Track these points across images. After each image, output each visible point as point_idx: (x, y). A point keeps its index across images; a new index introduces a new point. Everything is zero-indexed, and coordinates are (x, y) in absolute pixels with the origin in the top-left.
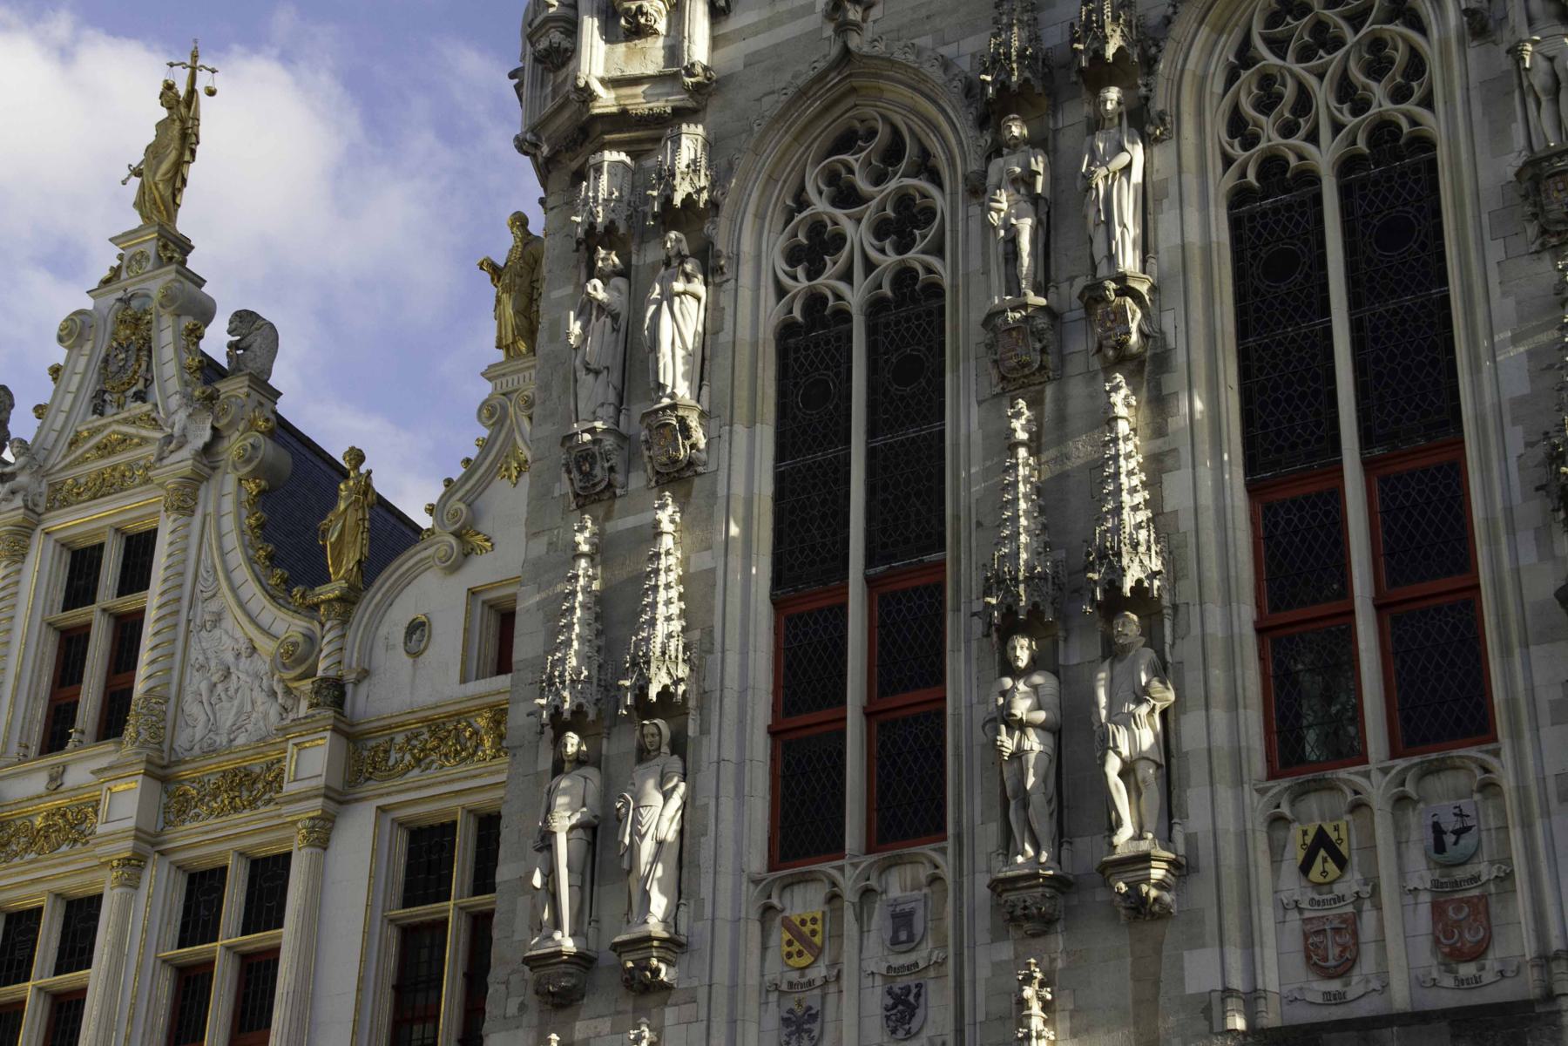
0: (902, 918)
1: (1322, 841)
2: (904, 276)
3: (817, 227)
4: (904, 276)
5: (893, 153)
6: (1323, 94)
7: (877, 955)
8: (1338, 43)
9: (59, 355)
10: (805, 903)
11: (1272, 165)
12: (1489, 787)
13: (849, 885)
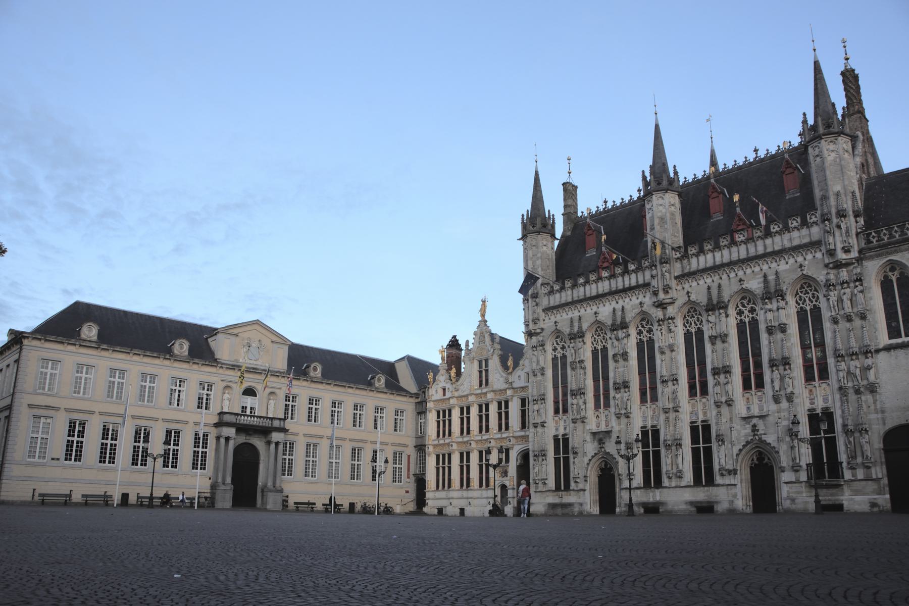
0: (565, 421)
1: (598, 416)
3: (555, 347)
5: (562, 340)
9: (474, 336)
10: (556, 418)
11: (595, 347)
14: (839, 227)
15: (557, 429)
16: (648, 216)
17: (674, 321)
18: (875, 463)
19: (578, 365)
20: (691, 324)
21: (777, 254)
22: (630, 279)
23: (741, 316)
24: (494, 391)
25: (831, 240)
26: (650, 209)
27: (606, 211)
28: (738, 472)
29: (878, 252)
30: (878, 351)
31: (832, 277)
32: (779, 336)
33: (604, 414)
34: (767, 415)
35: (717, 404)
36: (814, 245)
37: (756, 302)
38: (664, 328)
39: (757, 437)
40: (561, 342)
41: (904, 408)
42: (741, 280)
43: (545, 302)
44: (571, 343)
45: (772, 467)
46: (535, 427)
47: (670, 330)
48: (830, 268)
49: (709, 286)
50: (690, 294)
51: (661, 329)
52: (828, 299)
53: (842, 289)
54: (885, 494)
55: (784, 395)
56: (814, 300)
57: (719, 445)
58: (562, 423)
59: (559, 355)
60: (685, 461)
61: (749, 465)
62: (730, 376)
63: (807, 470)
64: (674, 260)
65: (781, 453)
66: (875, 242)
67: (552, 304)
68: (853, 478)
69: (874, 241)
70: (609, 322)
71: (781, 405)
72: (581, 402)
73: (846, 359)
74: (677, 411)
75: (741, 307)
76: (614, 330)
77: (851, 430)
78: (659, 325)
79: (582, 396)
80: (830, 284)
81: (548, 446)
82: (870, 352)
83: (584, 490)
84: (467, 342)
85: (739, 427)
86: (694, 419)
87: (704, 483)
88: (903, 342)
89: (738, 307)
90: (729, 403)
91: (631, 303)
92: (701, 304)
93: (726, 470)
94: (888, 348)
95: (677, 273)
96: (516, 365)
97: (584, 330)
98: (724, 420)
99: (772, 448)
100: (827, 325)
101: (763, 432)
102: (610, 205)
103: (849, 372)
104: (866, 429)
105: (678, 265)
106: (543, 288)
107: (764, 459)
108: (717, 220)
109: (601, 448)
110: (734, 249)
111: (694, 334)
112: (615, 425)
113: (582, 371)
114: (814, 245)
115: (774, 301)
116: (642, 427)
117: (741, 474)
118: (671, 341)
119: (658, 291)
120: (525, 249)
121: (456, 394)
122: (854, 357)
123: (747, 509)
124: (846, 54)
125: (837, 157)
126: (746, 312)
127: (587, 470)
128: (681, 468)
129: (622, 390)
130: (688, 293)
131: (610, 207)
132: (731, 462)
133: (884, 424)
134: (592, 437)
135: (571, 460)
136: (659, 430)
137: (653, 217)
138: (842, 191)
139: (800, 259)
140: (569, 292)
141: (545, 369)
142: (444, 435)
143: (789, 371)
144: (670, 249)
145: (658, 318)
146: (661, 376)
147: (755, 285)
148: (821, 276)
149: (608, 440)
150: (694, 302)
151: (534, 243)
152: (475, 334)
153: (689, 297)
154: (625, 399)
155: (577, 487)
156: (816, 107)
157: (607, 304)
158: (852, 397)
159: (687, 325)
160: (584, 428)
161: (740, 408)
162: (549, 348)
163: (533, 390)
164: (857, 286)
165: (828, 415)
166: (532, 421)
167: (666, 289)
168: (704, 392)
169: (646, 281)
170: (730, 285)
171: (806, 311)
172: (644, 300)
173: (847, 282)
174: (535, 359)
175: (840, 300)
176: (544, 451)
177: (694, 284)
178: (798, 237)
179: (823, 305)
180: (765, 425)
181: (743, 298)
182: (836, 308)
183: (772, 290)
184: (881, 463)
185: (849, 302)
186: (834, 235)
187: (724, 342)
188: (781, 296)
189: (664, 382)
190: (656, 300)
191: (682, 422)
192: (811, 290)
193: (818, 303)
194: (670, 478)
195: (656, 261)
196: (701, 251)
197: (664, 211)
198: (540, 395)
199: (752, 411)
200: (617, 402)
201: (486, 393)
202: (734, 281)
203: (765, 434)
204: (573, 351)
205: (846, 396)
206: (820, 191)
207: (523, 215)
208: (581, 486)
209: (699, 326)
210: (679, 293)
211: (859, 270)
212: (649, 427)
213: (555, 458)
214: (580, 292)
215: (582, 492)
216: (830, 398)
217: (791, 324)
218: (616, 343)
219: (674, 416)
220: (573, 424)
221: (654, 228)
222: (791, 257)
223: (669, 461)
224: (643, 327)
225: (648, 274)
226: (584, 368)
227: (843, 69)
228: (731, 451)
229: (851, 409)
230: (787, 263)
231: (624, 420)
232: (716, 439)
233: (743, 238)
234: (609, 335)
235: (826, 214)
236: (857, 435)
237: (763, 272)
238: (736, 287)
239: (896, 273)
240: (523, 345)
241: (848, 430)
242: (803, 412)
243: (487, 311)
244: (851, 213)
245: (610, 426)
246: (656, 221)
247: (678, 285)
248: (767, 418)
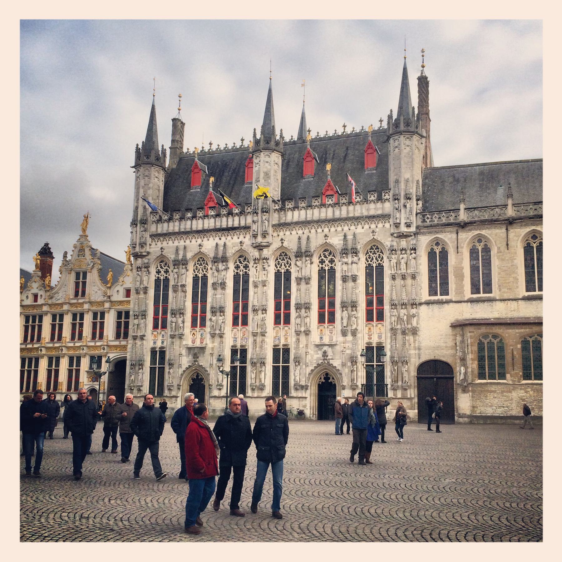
0: (163, 335)
1: (194, 333)
2: (166, 277)
4: (166, 277)
5: (166, 264)
6: (201, 269)
7: (161, 338)
8: (202, 265)
9: (74, 249)
10: (155, 333)
12: (205, 331)
13: (159, 332)
14: (405, 206)
15: (155, 343)
16: (255, 169)
17: (268, 261)
18: (410, 387)
19: (180, 288)
20: (281, 265)
21: (357, 220)
22: (233, 220)
23: (322, 265)
24: (91, 303)
25: (398, 216)
26: (258, 163)
27: (210, 153)
28: (309, 387)
29: (429, 230)
30: (421, 304)
31: (395, 244)
32: (350, 284)
33: (200, 334)
34: (335, 345)
35: (297, 332)
36: (384, 217)
37: (335, 255)
38: (259, 267)
39: (326, 362)
40: (165, 267)
41: (434, 348)
42: (326, 236)
43: (153, 228)
44: (174, 268)
46: (135, 338)
47: (264, 268)
49: (299, 237)
50: (283, 241)
51: (256, 267)
52: (390, 260)
53: (401, 254)
54: (415, 409)
55: (349, 330)
56: (379, 260)
57: (296, 366)
58: (160, 338)
59: (162, 278)
60: (266, 376)
61: (318, 383)
62: (309, 311)
63: (362, 388)
64: (273, 210)
65: (343, 375)
66: (428, 222)
67: (159, 231)
68: (394, 397)
69: (428, 221)
70: (212, 255)
71: (347, 337)
72: (180, 320)
73: (398, 307)
74: (265, 336)
75: (323, 258)
76: (215, 262)
77: (396, 361)
78: (255, 263)
79: (181, 315)
80: (393, 249)
81: (145, 357)
82: (416, 304)
83: (177, 397)
84: (66, 253)
85: (312, 352)
86: (277, 342)
88: (439, 299)
89: (321, 257)
90: (307, 333)
91: (232, 241)
92: (293, 250)
93: (300, 385)
94: (428, 303)
95: (275, 222)
96: (115, 280)
97: (188, 259)
98: (301, 346)
99: (337, 370)
100: (387, 280)
101: (331, 358)
102: (214, 148)
103: (399, 317)
104: (407, 361)
105: (276, 215)
106: (152, 216)
107: (329, 378)
108: (308, 181)
109: (195, 361)
110: (323, 210)
111: (283, 274)
112: (209, 343)
113: (183, 294)
114: (384, 217)
115: (350, 256)
116: (232, 346)
117: (310, 388)
118: (265, 279)
119: (257, 234)
120: (137, 178)
121: (50, 302)
122: (403, 307)
123: (313, 417)
124: (423, 63)
125: (410, 151)
126: (327, 262)
127: (181, 380)
128: (263, 382)
129: (218, 314)
130: (282, 240)
131: (214, 150)
132: (304, 379)
133: (419, 358)
134: (187, 351)
135: (167, 370)
136: (247, 349)
137: (258, 172)
138: (410, 179)
139: (373, 226)
140: (177, 223)
141: (148, 289)
142: (32, 339)
143: (355, 313)
144: (271, 201)
145: (255, 257)
146: (253, 306)
147: (336, 241)
148: (387, 242)
149: (202, 355)
150: (286, 248)
151: (147, 173)
152: (75, 247)
153: (282, 243)
154: (220, 322)
155: (170, 394)
156: (400, 108)
157: (211, 239)
158: (400, 337)
159: (278, 266)
160: (180, 343)
161: (315, 337)
162: (153, 270)
163: (134, 307)
164: (412, 254)
165: (380, 348)
166: (131, 333)
167: (264, 235)
168: (287, 321)
169: (247, 225)
170: (316, 238)
171: (373, 267)
172: (244, 240)
173: (405, 250)
174: (139, 278)
175: (398, 263)
176: (142, 361)
177: (288, 233)
178: (374, 209)
179: (386, 264)
180: (333, 352)
181: (325, 251)
182: (395, 268)
183: (350, 247)
184: (415, 387)
185: (405, 265)
186: (400, 212)
188: (356, 253)
189: (255, 311)
190: (254, 242)
191: (266, 345)
192: (378, 252)
193: (382, 262)
194: (253, 390)
195: (258, 209)
196: (296, 207)
197: (269, 167)
198: (142, 311)
200: (212, 323)
201: (83, 303)
202: (321, 236)
203: (332, 359)
204: (176, 276)
205: (394, 335)
206: (394, 176)
207: (137, 145)
208: (174, 393)
209: (288, 268)
210: (274, 238)
211: (414, 242)
212: (239, 347)
213: (151, 368)
214: (187, 225)
215: (174, 399)
216: (383, 336)
217: (360, 276)
218: (216, 274)
219: (261, 340)
220: (171, 339)
221: (259, 181)
222: (366, 224)
223: (253, 376)
224: (240, 262)
225: (249, 219)
226: (185, 292)
227: (419, 75)
228: (304, 371)
229: (397, 345)
230: (363, 228)
231: (217, 339)
232: (294, 360)
233: (332, 202)
234: (210, 266)
235: (397, 195)
236: (400, 364)
237: (344, 231)
238: (321, 241)
239: (440, 247)
240: (124, 263)
241: (394, 361)
242: (362, 345)
243: (88, 226)
244: (414, 197)
245: (204, 343)
246: (262, 175)
247: (274, 231)
248: (335, 347)
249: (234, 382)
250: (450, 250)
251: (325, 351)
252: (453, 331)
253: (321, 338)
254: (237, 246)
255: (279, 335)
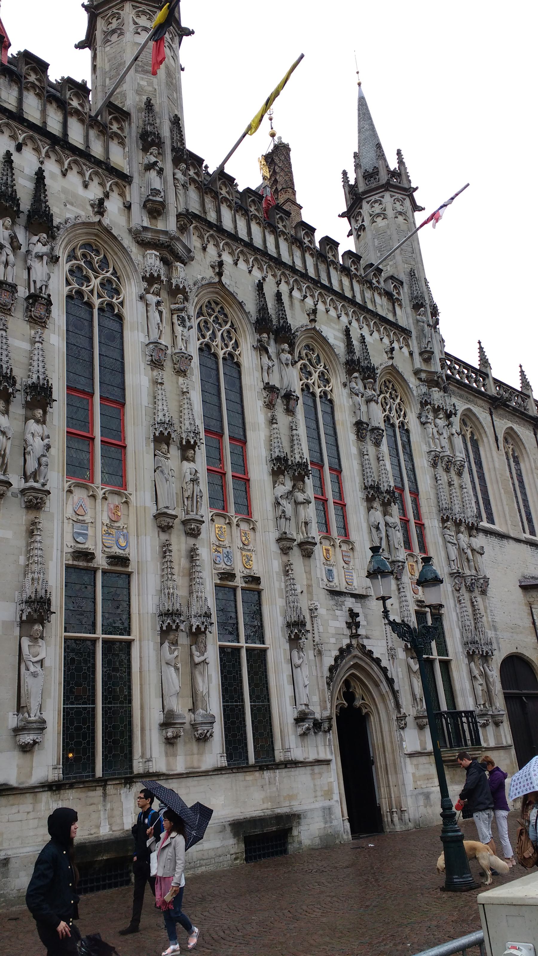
45: (367, 714)
48: (420, 379)
51: (158, 303)
78: (147, 291)
87: (252, 759)
103: (461, 551)
153: (220, 274)
187: (290, 411)
190: (145, 224)
194: (170, 742)
199: (336, 580)
249: (78, 712)
250: (485, 439)
251: (351, 610)
252: (525, 596)
253: (330, 571)
254: (84, 209)
255: (226, 543)
